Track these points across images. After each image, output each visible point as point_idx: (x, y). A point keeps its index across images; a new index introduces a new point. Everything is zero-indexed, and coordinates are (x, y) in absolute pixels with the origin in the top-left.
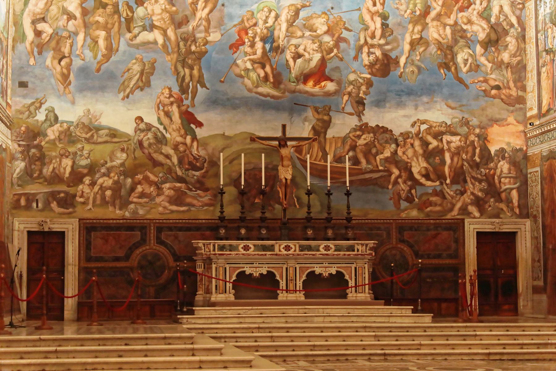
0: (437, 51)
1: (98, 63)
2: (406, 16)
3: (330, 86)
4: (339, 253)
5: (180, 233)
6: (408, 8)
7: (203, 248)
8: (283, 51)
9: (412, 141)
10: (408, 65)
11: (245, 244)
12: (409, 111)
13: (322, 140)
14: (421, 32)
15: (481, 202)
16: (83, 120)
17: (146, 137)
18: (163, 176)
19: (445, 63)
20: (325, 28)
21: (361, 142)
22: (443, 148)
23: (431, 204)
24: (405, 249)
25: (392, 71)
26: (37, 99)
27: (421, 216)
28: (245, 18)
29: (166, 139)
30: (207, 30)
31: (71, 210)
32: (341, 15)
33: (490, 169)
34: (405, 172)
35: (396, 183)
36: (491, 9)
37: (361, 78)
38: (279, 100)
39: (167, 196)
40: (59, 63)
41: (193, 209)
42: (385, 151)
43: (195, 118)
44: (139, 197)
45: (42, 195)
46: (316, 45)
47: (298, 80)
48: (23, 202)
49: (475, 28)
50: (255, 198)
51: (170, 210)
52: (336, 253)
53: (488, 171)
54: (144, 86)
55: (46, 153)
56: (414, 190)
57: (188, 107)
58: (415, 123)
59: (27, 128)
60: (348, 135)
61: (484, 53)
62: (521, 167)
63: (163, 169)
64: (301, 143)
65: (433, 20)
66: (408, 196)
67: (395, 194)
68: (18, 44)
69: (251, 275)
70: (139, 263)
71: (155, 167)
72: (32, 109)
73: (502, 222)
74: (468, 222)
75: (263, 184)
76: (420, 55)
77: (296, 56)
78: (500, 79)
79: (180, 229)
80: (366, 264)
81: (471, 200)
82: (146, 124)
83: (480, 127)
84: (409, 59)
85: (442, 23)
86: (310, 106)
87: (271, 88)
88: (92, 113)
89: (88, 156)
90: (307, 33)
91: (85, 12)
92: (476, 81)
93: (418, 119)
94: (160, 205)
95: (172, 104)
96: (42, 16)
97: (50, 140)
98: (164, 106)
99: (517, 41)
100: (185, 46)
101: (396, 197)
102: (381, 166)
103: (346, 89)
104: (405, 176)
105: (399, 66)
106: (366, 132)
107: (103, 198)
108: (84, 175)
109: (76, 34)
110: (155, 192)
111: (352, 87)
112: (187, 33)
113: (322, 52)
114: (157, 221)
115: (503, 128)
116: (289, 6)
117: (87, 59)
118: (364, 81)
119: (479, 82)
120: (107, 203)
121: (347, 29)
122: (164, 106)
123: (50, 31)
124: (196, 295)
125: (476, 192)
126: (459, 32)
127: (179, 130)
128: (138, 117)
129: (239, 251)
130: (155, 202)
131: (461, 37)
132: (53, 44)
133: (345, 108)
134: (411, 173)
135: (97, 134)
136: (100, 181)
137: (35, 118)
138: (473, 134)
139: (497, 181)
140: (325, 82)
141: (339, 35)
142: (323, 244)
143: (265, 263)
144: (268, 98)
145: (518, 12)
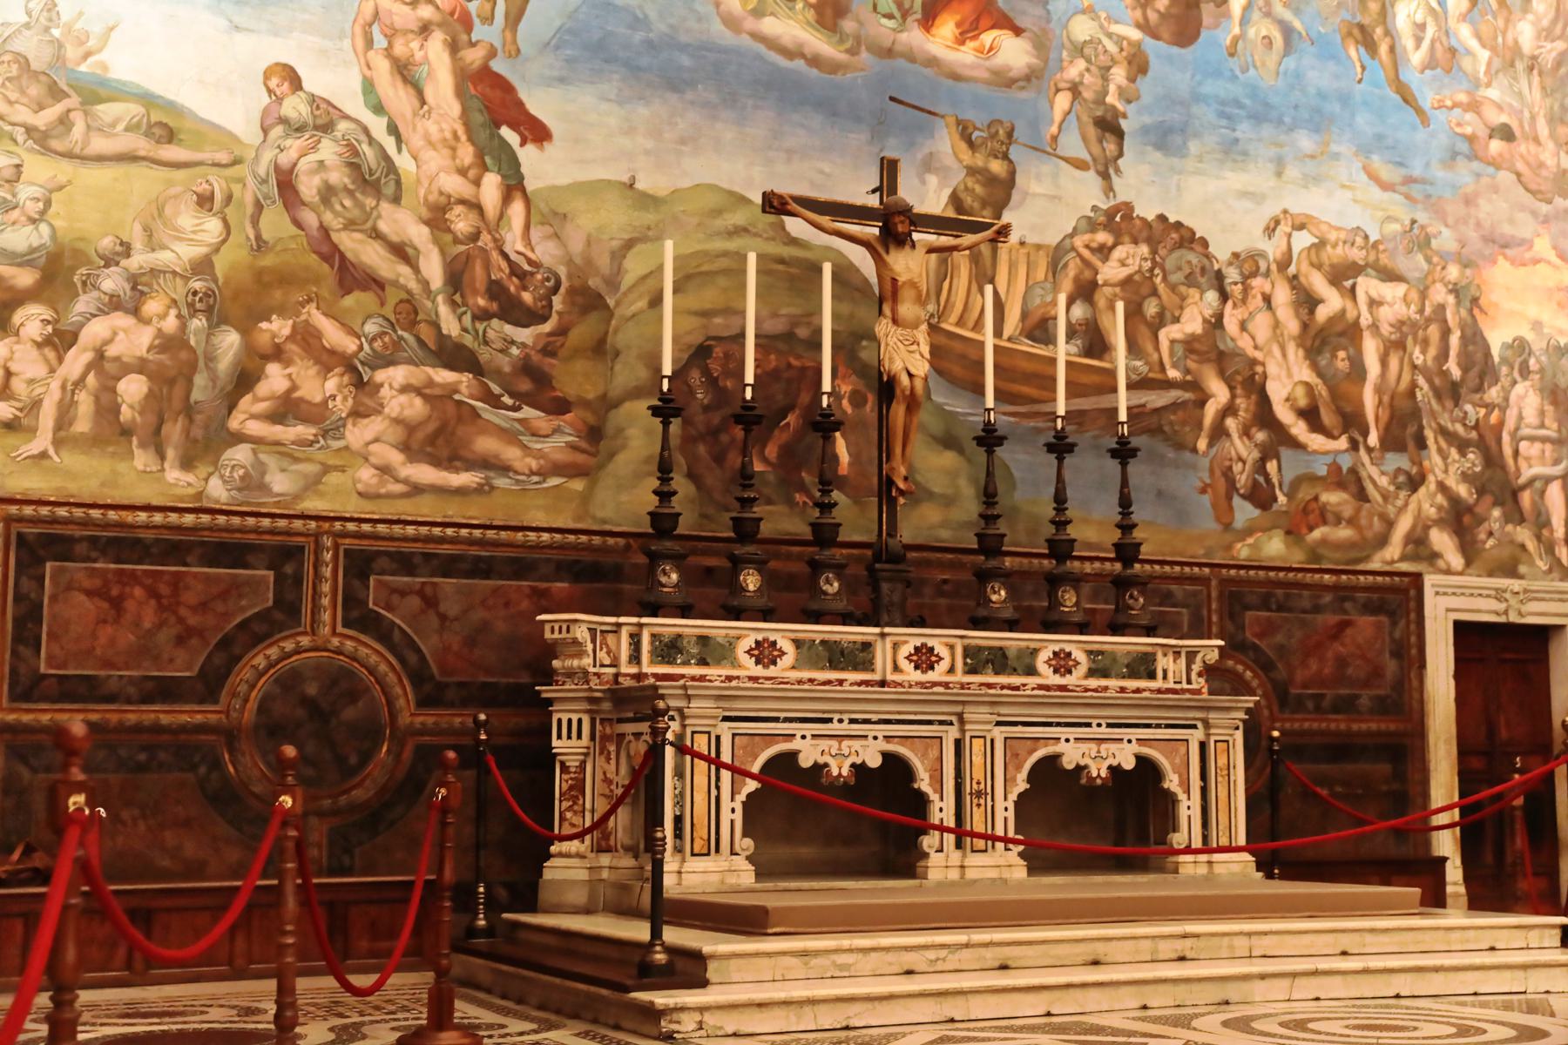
3: (1013, 52)
4: (1103, 682)
5: (448, 584)
7: (590, 647)
9: (1267, 288)
10: (1256, 15)
11: (760, 638)
12: (1256, 177)
15: (1467, 519)
17: (313, 157)
18: (381, 335)
19: (1362, 27)
21: (1111, 272)
22: (1356, 323)
23: (1324, 516)
24: (1249, 674)
25: (1208, 28)
27: (1297, 558)
29: (398, 175)
33: (1490, 407)
34: (1248, 397)
35: (1219, 432)
37: (1110, 35)
38: (839, 77)
39: (397, 421)
41: (501, 482)
43: (520, 104)
51: (406, 481)
52: (1093, 683)
53: (1482, 411)
56: (1275, 462)
57: (492, 53)
60: (1068, 241)
63: (382, 304)
66: (1255, 483)
67: (1218, 473)
69: (818, 768)
70: (262, 708)
71: (349, 292)
73: (1526, 591)
74: (1433, 586)
78: (1511, 106)
79: (449, 566)
80: (1237, 728)
81: (1440, 508)
82: (313, 100)
86: (943, 117)
87: (808, 23)
88: (65, 18)
89: (43, 213)
92: (1449, 103)
93: (1285, 212)
94: (366, 460)
95: (425, 29)
101: (1221, 484)
102: (1174, 366)
103: (1062, 69)
104: (1246, 411)
105: (1228, 15)
106: (1126, 239)
107: (107, 408)
108: (20, 298)
110: (345, 399)
111: (1081, 64)
114: (351, 526)
115: (1522, 270)
118: (1122, 50)
119: (1455, 105)
120: (126, 432)
122: (391, 34)
124: (549, 856)
125: (1452, 482)
128: (277, 64)
129: (735, 664)
130: (341, 444)
133: (1061, 139)
134: (1264, 401)
135: (86, 113)
136: (96, 330)
138: (1442, 280)
139: (1507, 451)
140: (995, 33)
142: (1049, 644)
143: (874, 717)
144: (799, 64)
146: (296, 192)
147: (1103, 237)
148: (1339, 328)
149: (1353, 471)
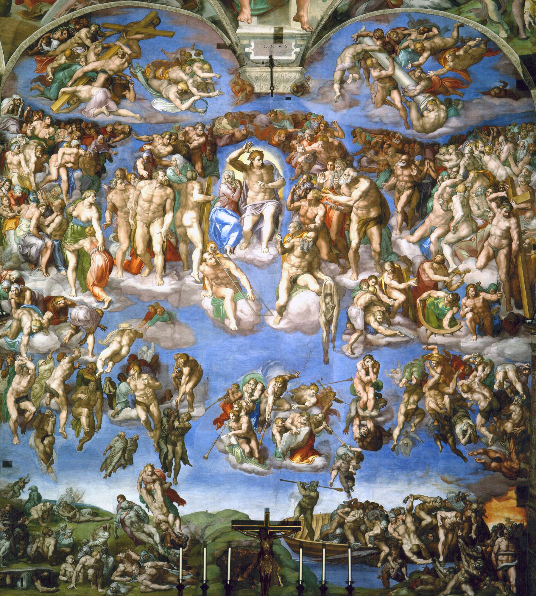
0: (433, 423)
1: (80, 441)
2: (401, 385)
3: (318, 461)
6: (403, 377)
8: (269, 425)
9: (404, 518)
10: (402, 438)
13: (309, 517)
14: (417, 402)
15: (476, 581)
16: (65, 499)
19: (442, 435)
20: (313, 400)
22: (437, 525)
23: (423, 582)
26: (21, 479)
28: (230, 392)
30: (191, 406)
31: (54, 588)
32: (330, 385)
35: (385, 560)
37: (351, 451)
38: (265, 477)
39: (149, 575)
40: (42, 442)
42: (375, 528)
43: (178, 496)
44: (121, 576)
45: (26, 573)
46: (304, 418)
47: (284, 455)
48: (8, 581)
49: (476, 396)
50: (238, 576)
51: (152, 588)
53: (484, 548)
54: (126, 464)
55: (30, 532)
57: (171, 484)
58: (408, 498)
59: (12, 507)
61: (485, 423)
62: (521, 544)
65: (430, 389)
68: (2, 423)
72: (16, 488)
76: (415, 426)
77: (284, 430)
78: (501, 451)
81: (466, 578)
82: (128, 502)
83: (477, 502)
84: (403, 431)
85: (440, 391)
90: (295, 406)
91: (68, 390)
92: (475, 453)
93: (411, 495)
95: (154, 481)
96: (25, 394)
97: (34, 519)
98: (146, 485)
100: (168, 422)
101: (386, 575)
109: (59, 412)
111: (341, 461)
112: (170, 408)
113: (310, 425)
116: (276, 378)
117: (70, 437)
119: (478, 454)
120: (90, 581)
121: (337, 401)
123: (33, 409)
125: (471, 570)
126: (458, 401)
127: (161, 508)
131: (461, 407)
132: (36, 423)
133: (334, 484)
136: (83, 560)
137: (19, 498)
138: (470, 509)
139: (494, 559)
141: (329, 407)
144: (253, 475)
145: (523, 378)
146: (125, 524)
147: (347, 509)
148: (430, 527)
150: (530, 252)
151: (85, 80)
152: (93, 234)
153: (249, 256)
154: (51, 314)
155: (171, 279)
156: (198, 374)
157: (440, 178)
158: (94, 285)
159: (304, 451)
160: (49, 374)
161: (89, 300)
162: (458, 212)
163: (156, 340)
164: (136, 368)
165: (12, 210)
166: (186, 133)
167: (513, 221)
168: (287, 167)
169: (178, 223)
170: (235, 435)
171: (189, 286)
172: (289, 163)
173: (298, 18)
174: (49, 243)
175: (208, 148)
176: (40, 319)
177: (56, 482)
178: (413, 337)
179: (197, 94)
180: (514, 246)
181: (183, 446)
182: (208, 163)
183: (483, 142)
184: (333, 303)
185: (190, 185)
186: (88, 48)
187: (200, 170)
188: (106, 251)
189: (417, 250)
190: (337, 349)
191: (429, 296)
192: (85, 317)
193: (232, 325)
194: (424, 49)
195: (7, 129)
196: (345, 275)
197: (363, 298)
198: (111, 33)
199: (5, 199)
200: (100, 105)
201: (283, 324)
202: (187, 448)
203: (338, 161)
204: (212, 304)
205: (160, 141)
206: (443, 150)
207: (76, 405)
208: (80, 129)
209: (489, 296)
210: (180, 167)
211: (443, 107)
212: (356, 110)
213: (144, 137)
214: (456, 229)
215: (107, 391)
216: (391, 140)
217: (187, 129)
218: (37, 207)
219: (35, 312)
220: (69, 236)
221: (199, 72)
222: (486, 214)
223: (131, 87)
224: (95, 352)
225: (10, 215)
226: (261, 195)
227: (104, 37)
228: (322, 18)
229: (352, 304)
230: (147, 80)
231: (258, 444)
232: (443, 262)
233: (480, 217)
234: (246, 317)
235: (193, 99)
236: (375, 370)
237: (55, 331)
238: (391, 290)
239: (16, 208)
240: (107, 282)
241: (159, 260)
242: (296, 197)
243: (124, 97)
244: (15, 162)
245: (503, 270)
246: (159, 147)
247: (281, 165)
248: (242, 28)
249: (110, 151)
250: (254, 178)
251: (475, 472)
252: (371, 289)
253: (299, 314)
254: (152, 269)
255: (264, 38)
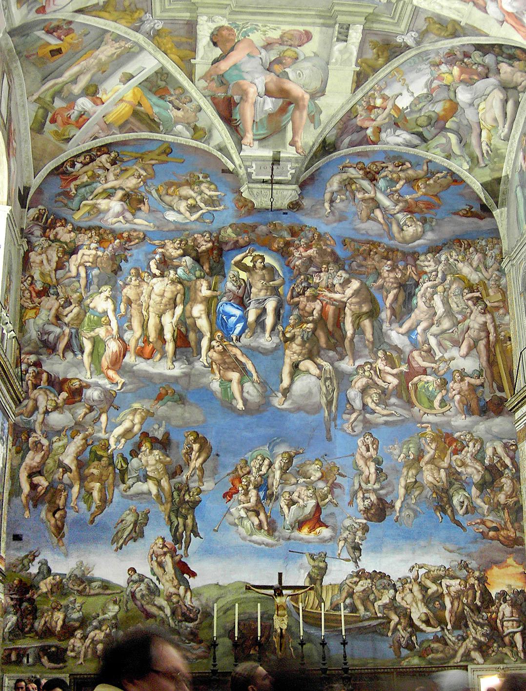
1: (91, 514)
2: (400, 460)
3: (325, 532)
6: (401, 452)
8: (277, 498)
9: (411, 587)
13: (318, 586)
15: (484, 648)
16: (75, 572)
20: (319, 475)
22: (442, 593)
23: (432, 651)
27: (423, 664)
28: (239, 467)
30: (201, 480)
32: (335, 460)
33: (492, 613)
35: (395, 629)
36: (484, 452)
49: (469, 470)
57: (182, 556)
64: (297, 592)
65: (427, 463)
75: (259, 634)
82: (139, 575)
83: (479, 569)
90: (301, 480)
95: (165, 554)
96: (38, 470)
98: (157, 558)
99: (512, 481)
109: (71, 486)
111: (347, 532)
116: (282, 454)
117: (81, 511)
119: (476, 524)
121: (340, 474)
123: (46, 484)
125: (478, 637)
126: (454, 474)
131: (456, 480)
132: (49, 496)
134: (411, 619)
139: (499, 625)
145: (511, 453)
147: (355, 579)
148: (436, 595)
149: (442, 637)
150: (506, 343)
151: (105, 195)
152: (109, 323)
153: (253, 344)
154: (67, 395)
155: (181, 364)
156: (207, 450)
157: (421, 280)
158: (108, 368)
159: (311, 524)
160: (63, 450)
161: (104, 382)
162: (440, 309)
163: (168, 419)
164: (148, 444)
165: (32, 302)
166: (195, 240)
167: (488, 316)
168: (286, 268)
169: (187, 314)
170: (244, 508)
171: (197, 370)
172: (288, 266)
173: (293, 143)
174: (67, 330)
175: (215, 252)
176: (56, 399)
177: (66, 555)
178: (407, 417)
179: (205, 209)
180: (492, 338)
181: (194, 519)
182: (215, 265)
183: (456, 252)
184: (333, 386)
185: (198, 282)
186: (108, 170)
187: (208, 270)
188: (121, 338)
189: (405, 339)
190: (338, 427)
191: (420, 380)
192: (99, 397)
193: (240, 406)
194: (400, 179)
195: (32, 234)
196: (343, 361)
197: (360, 382)
198: (128, 159)
199: (27, 292)
200: (118, 215)
201: (286, 406)
202: (197, 521)
203: (331, 265)
204: (220, 386)
205: (172, 246)
206: (422, 258)
207: (89, 480)
208: (99, 235)
209: (473, 381)
210: (190, 267)
211: (418, 223)
212: (345, 224)
213: (157, 242)
214: (439, 323)
215: (119, 466)
216: (377, 248)
217: (196, 236)
218: (57, 299)
219: (51, 392)
220: (86, 324)
221: (207, 191)
222: (464, 310)
223: (146, 201)
224: (108, 430)
225: (31, 305)
226: (263, 293)
227: (122, 161)
228: (314, 144)
229: (350, 386)
230: (160, 196)
231: (267, 517)
232: (430, 351)
233: (460, 313)
234: (252, 398)
235: (201, 212)
236: (374, 446)
237: (70, 410)
238: (385, 375)
239: (37, 300)
240: (121, 365)
241: (170, 347)
242: (294, 293)
243: (140, 209)
244: (38, 261)
245: (484, 358)
246: (170, 250)
247: (282, 268)
248: (245, 151)
249: (126, 253)
250: (257, 277)
251: (475, 541)
252: (367, 374)
253: (302, 395)
254: (164, 355)
255: (264, 161)
